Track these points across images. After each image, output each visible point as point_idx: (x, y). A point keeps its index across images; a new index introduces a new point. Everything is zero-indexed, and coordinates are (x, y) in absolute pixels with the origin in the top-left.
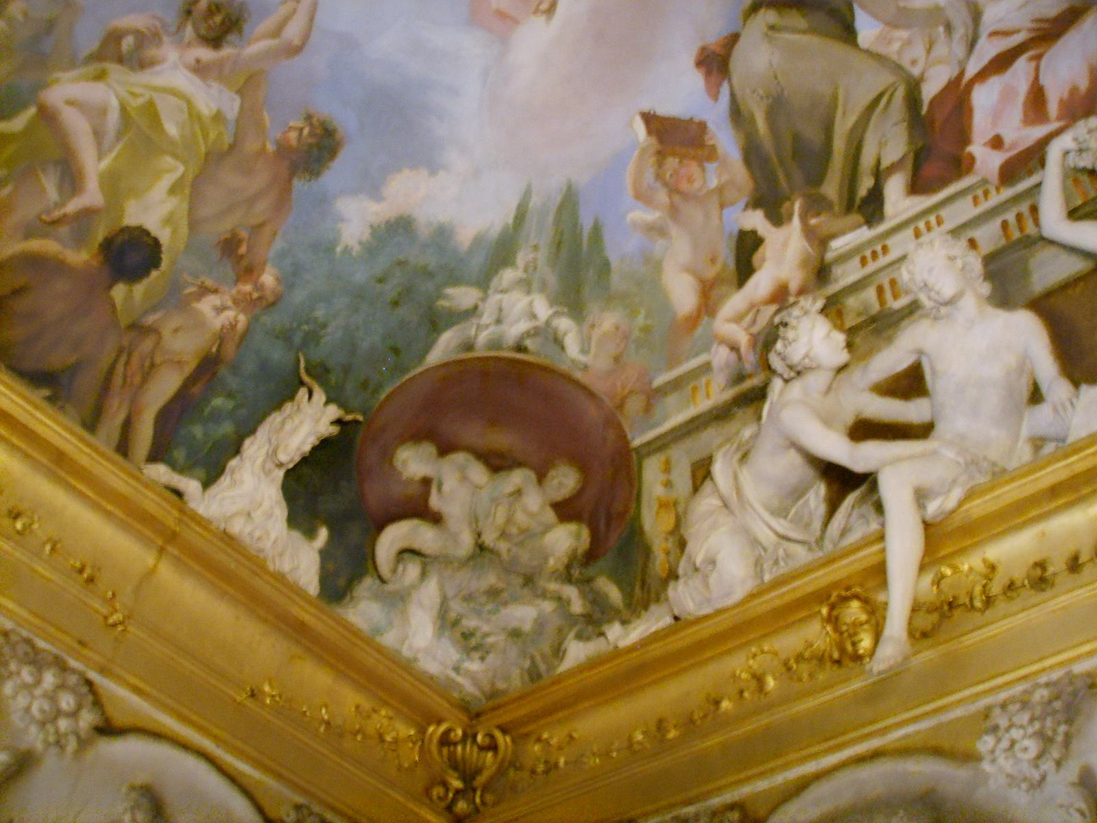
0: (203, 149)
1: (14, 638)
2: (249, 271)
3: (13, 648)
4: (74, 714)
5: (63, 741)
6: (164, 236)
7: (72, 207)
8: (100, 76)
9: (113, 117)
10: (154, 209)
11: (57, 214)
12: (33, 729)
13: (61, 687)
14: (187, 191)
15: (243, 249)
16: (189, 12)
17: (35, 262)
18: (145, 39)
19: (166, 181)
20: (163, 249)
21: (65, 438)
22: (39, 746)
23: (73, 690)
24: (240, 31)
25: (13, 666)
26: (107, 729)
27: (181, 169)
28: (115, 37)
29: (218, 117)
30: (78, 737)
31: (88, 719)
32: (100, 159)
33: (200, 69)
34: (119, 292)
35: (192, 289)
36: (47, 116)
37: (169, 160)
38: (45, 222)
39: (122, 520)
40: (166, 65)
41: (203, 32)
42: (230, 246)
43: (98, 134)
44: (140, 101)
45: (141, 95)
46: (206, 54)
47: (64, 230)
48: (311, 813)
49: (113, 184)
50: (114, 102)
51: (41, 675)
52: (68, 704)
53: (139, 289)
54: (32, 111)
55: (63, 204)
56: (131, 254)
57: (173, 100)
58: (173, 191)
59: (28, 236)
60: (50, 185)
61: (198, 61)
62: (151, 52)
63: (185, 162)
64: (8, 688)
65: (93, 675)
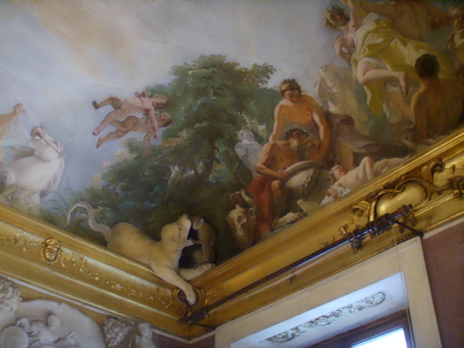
0: (389, 30)
2: (448, 20)
6: (423, 52)
7: (403, 84)
8: (356, 63)
9: (372, 60)
10: (411, 54)
11: (404, 89)
14: (407, 39)
15: (437, 20)
16: (335, 27)
17: (419, 104)
18: (343, 44)
19: (400, 46)
20: (429, 53)
21: (446, 145)
24: (343, 9)
27: (396, 40)
28: (342, 54)
29: (377, 21)
32: (387, 69)
33: (357, 26)
34: (441, 76)
35: (449, 47)
36: (367, 83)
37: (392, 44)
38: (406, 95)
39: (448, 160)
40: (355, 39)
41: (343, 23)
42: (434, 26)
43: (377, 67)
44: (367, 50)
45: (365, 49)
46: (351, 23)
47: (411, 89)
49: (398, 66)
50: (366, 59)
53: (442, 67)
54: (365, 87)
55: (401, 87)
56: (426, 67)
57: (367, 38)
58: (405, 45)
59: (410, 103)
60: (393, 89)
61: (354, 27)
62: (349, 41)
63: (393, 39)
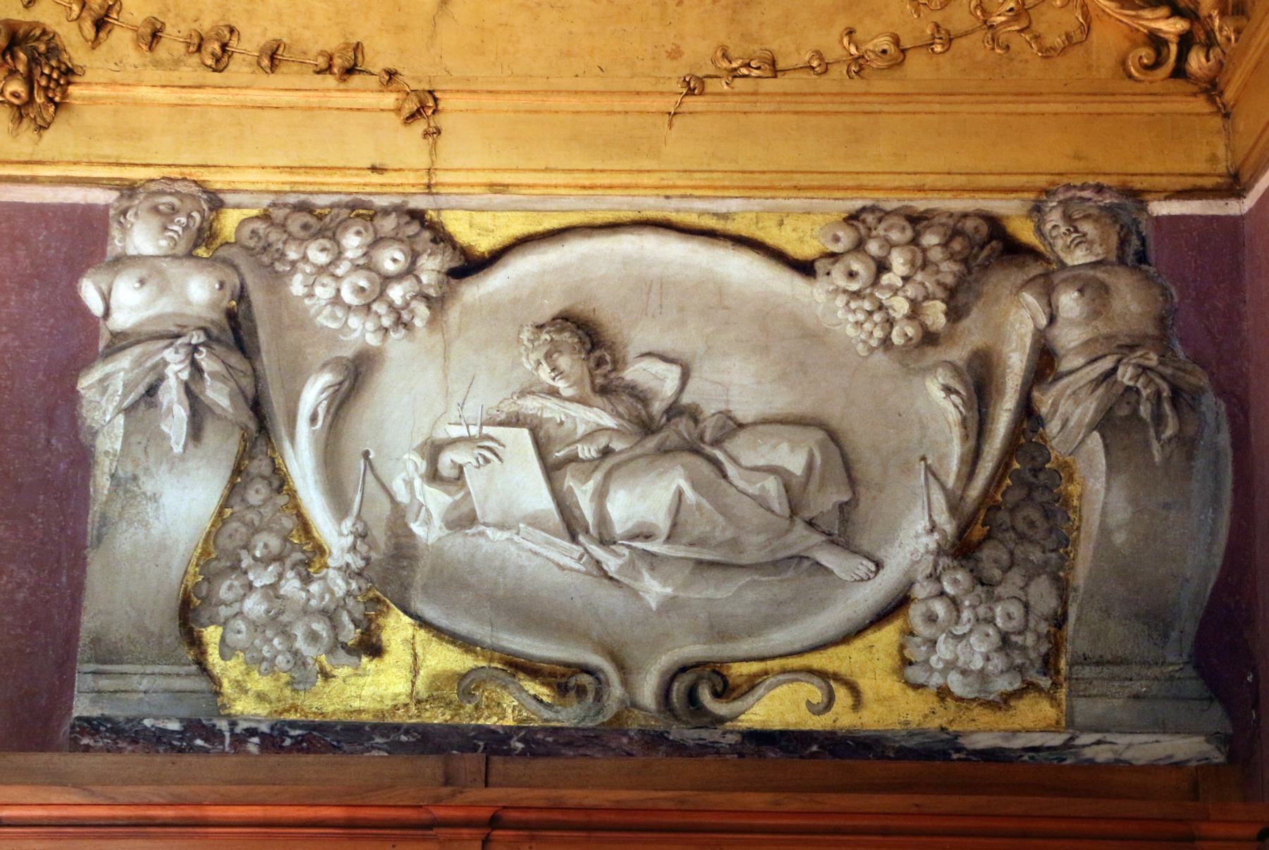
1: (278, 214)
3: (283, 226)
4: (410, 271)
5: (406, 316)
12: (354, 322)
13: (378, 241)
22: (373, 340)
23: (395, 239)
25: (292, 255)
26: (470, 265)
30: (427, 298)
31: (431, 266)
48: (882, 215)
51: (339, 244)
52: (395, 260)
64: (297, 286)
65: (417, 203)
